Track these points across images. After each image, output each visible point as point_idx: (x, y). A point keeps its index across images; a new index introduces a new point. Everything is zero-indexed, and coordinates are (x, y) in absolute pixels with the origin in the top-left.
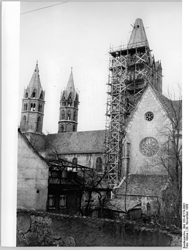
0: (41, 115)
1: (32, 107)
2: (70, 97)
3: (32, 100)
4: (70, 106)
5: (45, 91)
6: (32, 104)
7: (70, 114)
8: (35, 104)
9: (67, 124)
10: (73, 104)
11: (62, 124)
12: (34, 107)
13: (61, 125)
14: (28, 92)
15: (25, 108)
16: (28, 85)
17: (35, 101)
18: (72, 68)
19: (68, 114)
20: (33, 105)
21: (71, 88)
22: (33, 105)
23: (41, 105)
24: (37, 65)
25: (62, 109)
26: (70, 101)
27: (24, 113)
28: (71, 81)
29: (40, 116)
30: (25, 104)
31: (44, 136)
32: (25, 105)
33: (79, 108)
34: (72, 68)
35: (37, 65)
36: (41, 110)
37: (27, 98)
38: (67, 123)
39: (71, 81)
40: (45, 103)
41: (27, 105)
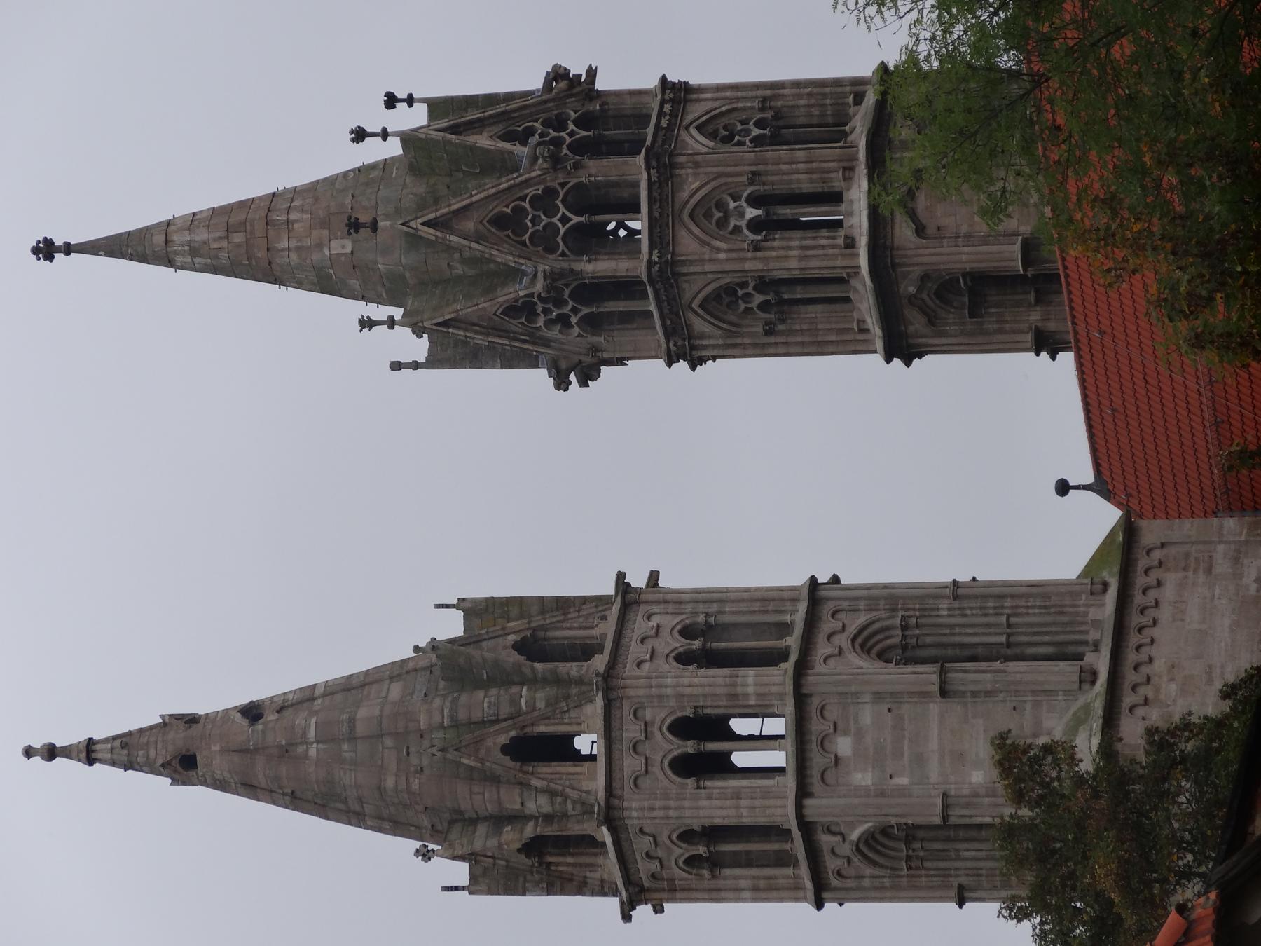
0: (828, 625)
1: (722, 766)
2: (500, 221)
3: (630, 765)
4: (634, 209)
5: (461, 604)
6: (685, 766)
7: (754, 201)
8: (682, 728)
9: (920, 230)
10: (598, 169)
11: (912, 299)
12: (717, 728)
13: (931, 321)
14: (512, 837)
15: (748, 861)
16: (417, 844)
17: (632, 731)
18: (46, 250)
19: (755, 225)
20: (690, 747)
21: (354, 226)
22: (690, 747)
23: (687, 632)
24: (89, 752)
25: (699, 325)
26: (564, 219)
27: (831, 864)
28: (242, 242)
29: (843, 640)
30: (692, 861)
31: (1125, 547)
32: (715, 863)
33: (650, 82)
34: (46, 250)
35: (89, 752)
36: (758, 629)
37: (605, 835)
38: (903, 232)
39: (242, 242)
40: (638, 580)
41: (713, 833)
